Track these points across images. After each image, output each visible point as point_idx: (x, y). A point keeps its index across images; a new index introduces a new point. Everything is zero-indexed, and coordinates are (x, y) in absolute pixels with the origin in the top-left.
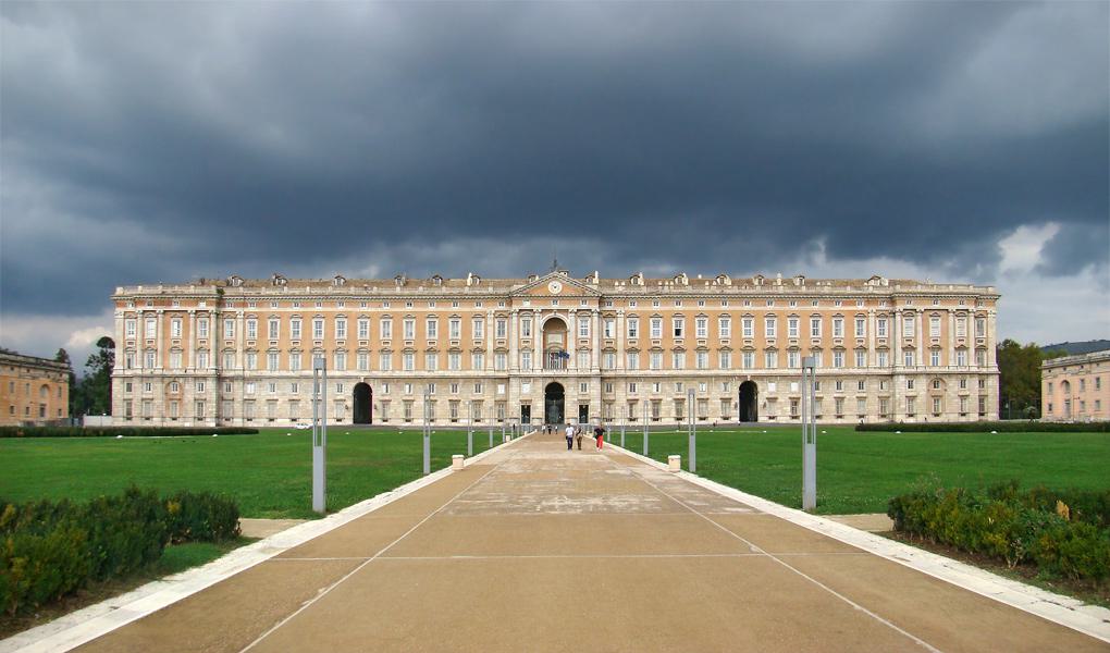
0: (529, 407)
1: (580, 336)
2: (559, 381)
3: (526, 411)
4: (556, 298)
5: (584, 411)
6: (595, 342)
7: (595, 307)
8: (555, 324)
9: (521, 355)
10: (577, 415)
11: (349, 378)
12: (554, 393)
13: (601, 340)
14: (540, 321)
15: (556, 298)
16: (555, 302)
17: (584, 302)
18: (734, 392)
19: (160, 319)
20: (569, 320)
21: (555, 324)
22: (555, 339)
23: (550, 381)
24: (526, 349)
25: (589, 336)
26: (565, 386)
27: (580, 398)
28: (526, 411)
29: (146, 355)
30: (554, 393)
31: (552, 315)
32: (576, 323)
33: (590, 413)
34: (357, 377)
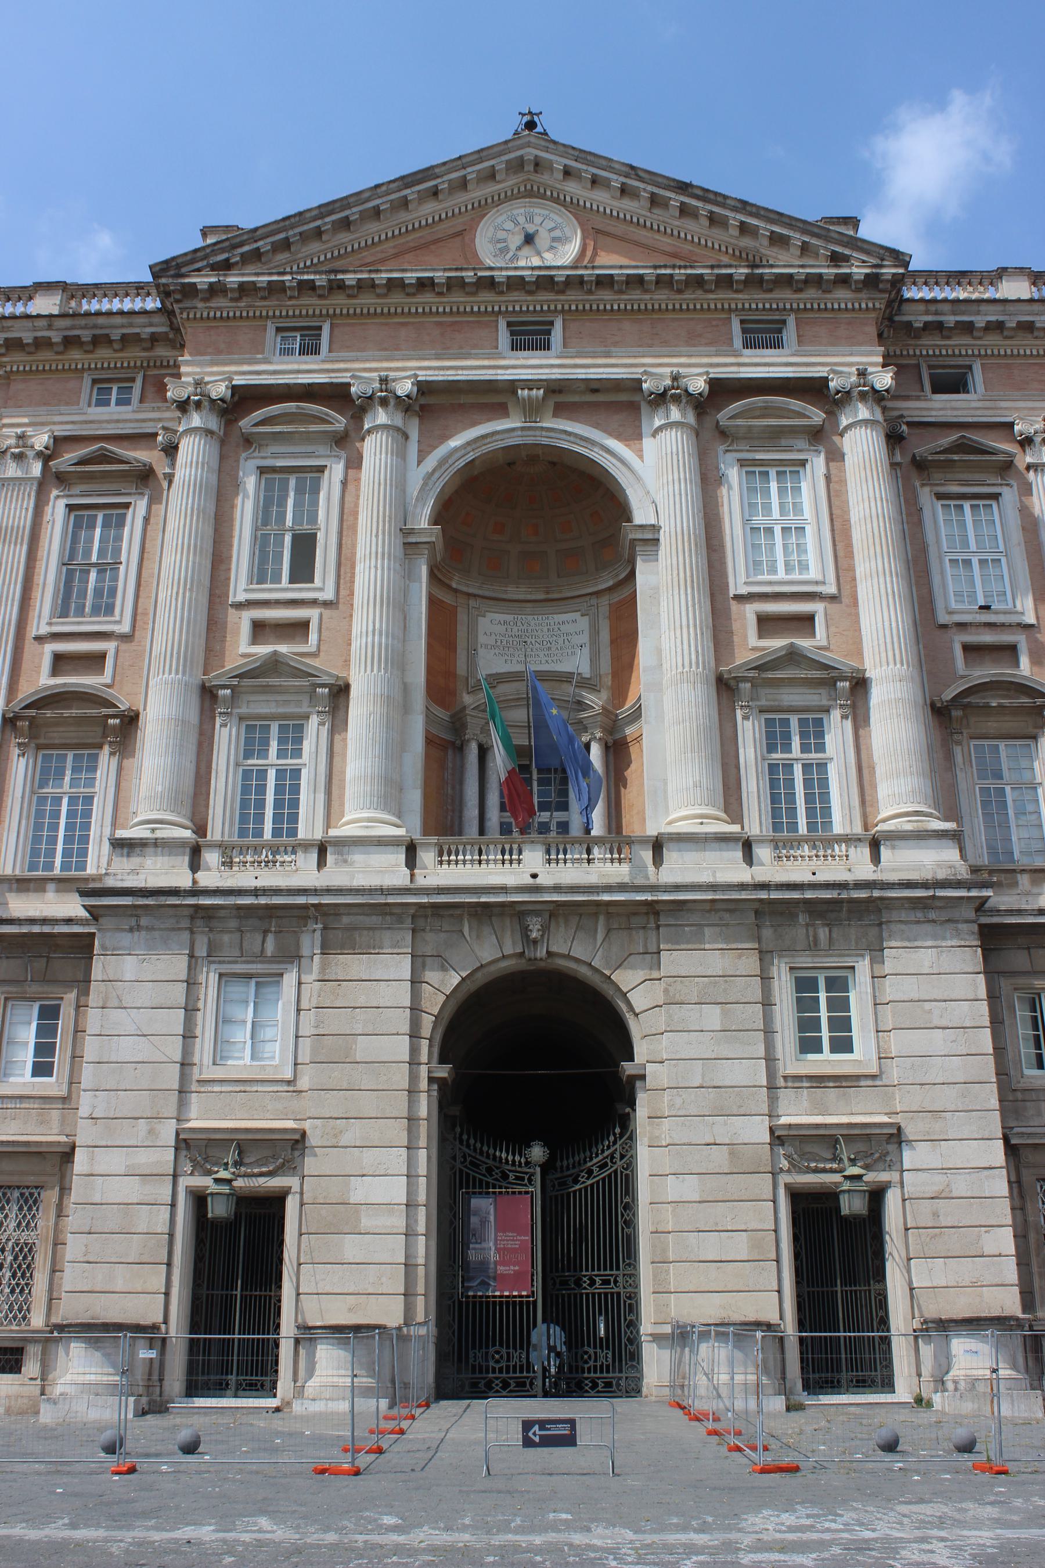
3: (237, 1254)
4: (533, 310)
7: (855, 362)
9: (226, 738)
10: (769, 1294)
12: (532, 1082)
15: (533, 310)
16: (530, 336)
17: (764, 334)
23: (490, 951)
24: (262, 692)
27: (799, 1112)
28: (237, 1254)
30: (532, 1082)
31: (505, 428)
32: (708, 481)
33: (915, 1280)
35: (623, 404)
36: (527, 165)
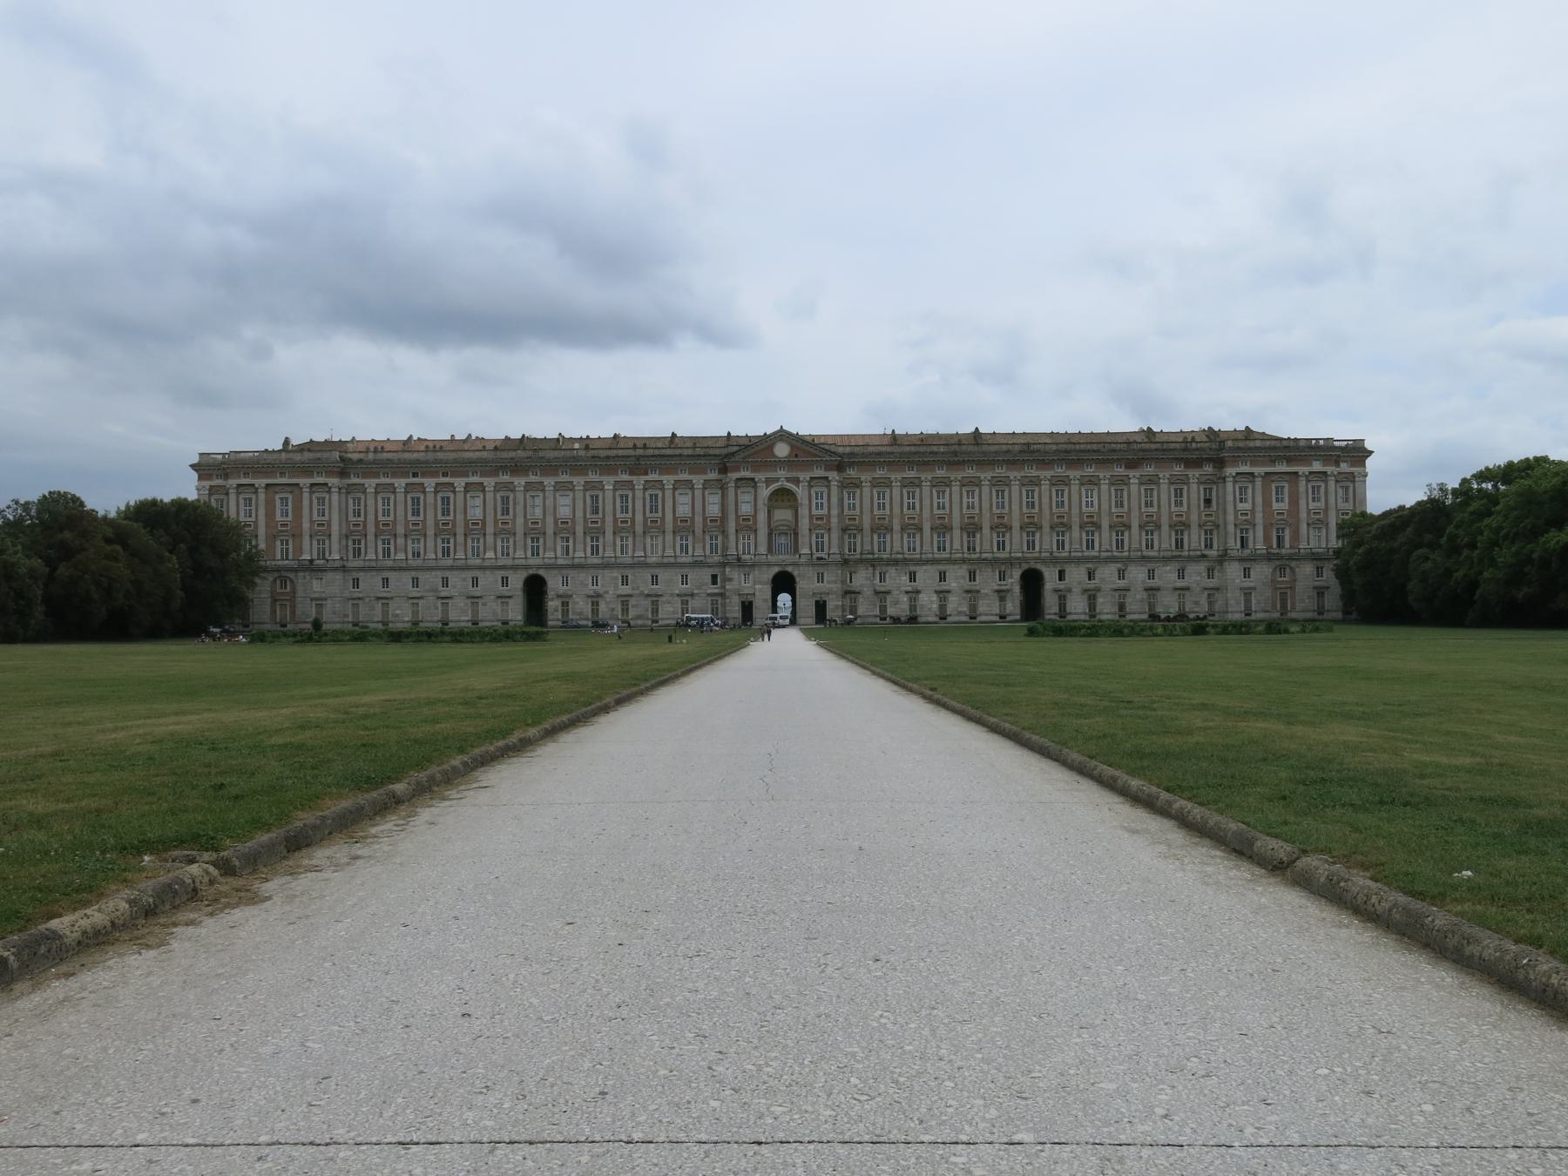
0: (751, 603)
1: (814, 512)
2: (789, 569)
5: (821, 608)
6: (834, 520)
8: (783, 496)
11: (514, 568)
14: (765, 492)
18: (1014, 580)
19: (262, 496)
20: (801, 492)
21: (783, 496)
22: (783, 515)
23: (776, 569)
25: (825, 512)
26: (795, 573)
29: (469, 541)
34: (527, 567)
35: (796, 481)
36: (782, 435)
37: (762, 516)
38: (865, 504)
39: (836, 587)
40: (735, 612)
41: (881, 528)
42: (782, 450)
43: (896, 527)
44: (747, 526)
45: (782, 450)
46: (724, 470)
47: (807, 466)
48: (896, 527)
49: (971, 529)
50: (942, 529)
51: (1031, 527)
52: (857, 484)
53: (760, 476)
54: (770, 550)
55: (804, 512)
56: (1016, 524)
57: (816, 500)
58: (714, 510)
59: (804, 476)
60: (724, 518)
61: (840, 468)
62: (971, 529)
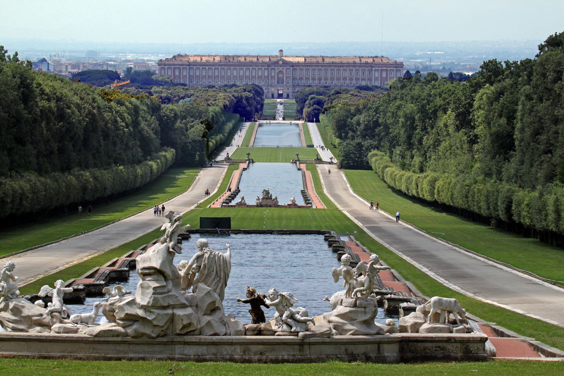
13: (293, 76)
20: (284, 71)
21: (281, 72)
22: (281, 75)
37: (276, 76)
38: (298, 74)
39: (291, 91)
40: (270, 96)
41: (301, 79)
42: (281, 62)
43: (304, 78)
44: (273, 77)
45: (281, 62)
46: (268, 66)
47: (286, 66)
48: (304, 78)
49: (320, 79)
50: (314, 79)
51: (332, 79)
52: (296, 69)
53: (276, 68)
54: (278, 83)
55: (285, 75)
56: (329, 79)
57: (287, 73)
58: (266, 74)
59: (285, 68)
60: (268, 76)
61: (293, 66)
62: (320, 79)
